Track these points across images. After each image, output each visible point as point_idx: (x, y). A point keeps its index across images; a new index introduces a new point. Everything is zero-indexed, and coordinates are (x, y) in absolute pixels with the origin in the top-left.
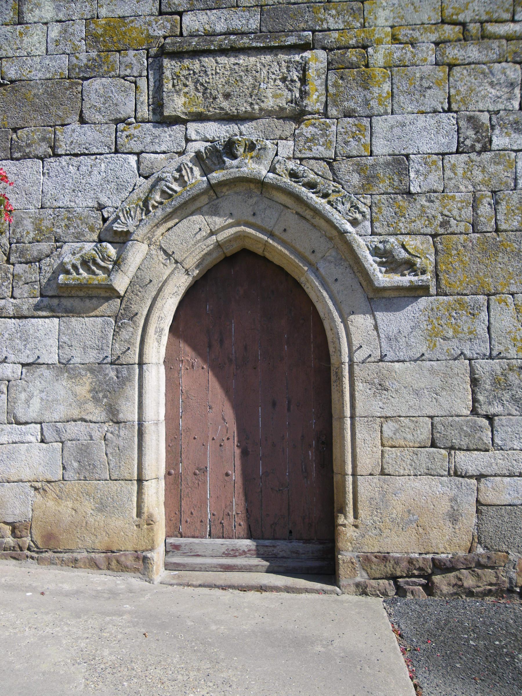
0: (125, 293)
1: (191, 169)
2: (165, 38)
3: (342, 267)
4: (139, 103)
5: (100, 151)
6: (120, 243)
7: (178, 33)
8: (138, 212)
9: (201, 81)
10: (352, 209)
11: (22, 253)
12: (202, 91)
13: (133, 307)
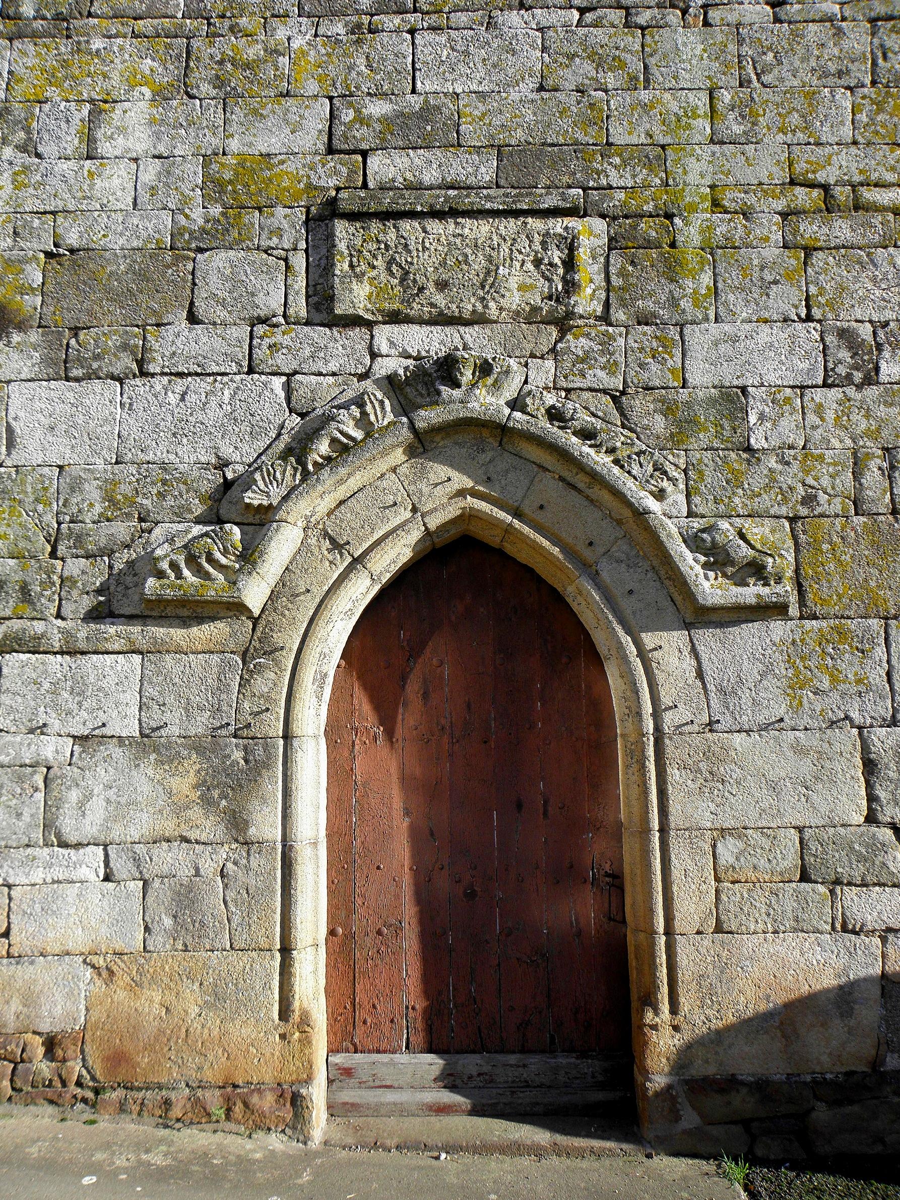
0: (263, 611)
1: (382, 403)
2: (338, 189)
3: (640, 570)
4: (291, 292)
5: (223, 370)
6: (255, 525)
7: (360, 184)
8: (287, 473)
9: (398, 260)
10: (657, 473)
11: (79, 540)
12: (398, 276)
13: (275, 635)
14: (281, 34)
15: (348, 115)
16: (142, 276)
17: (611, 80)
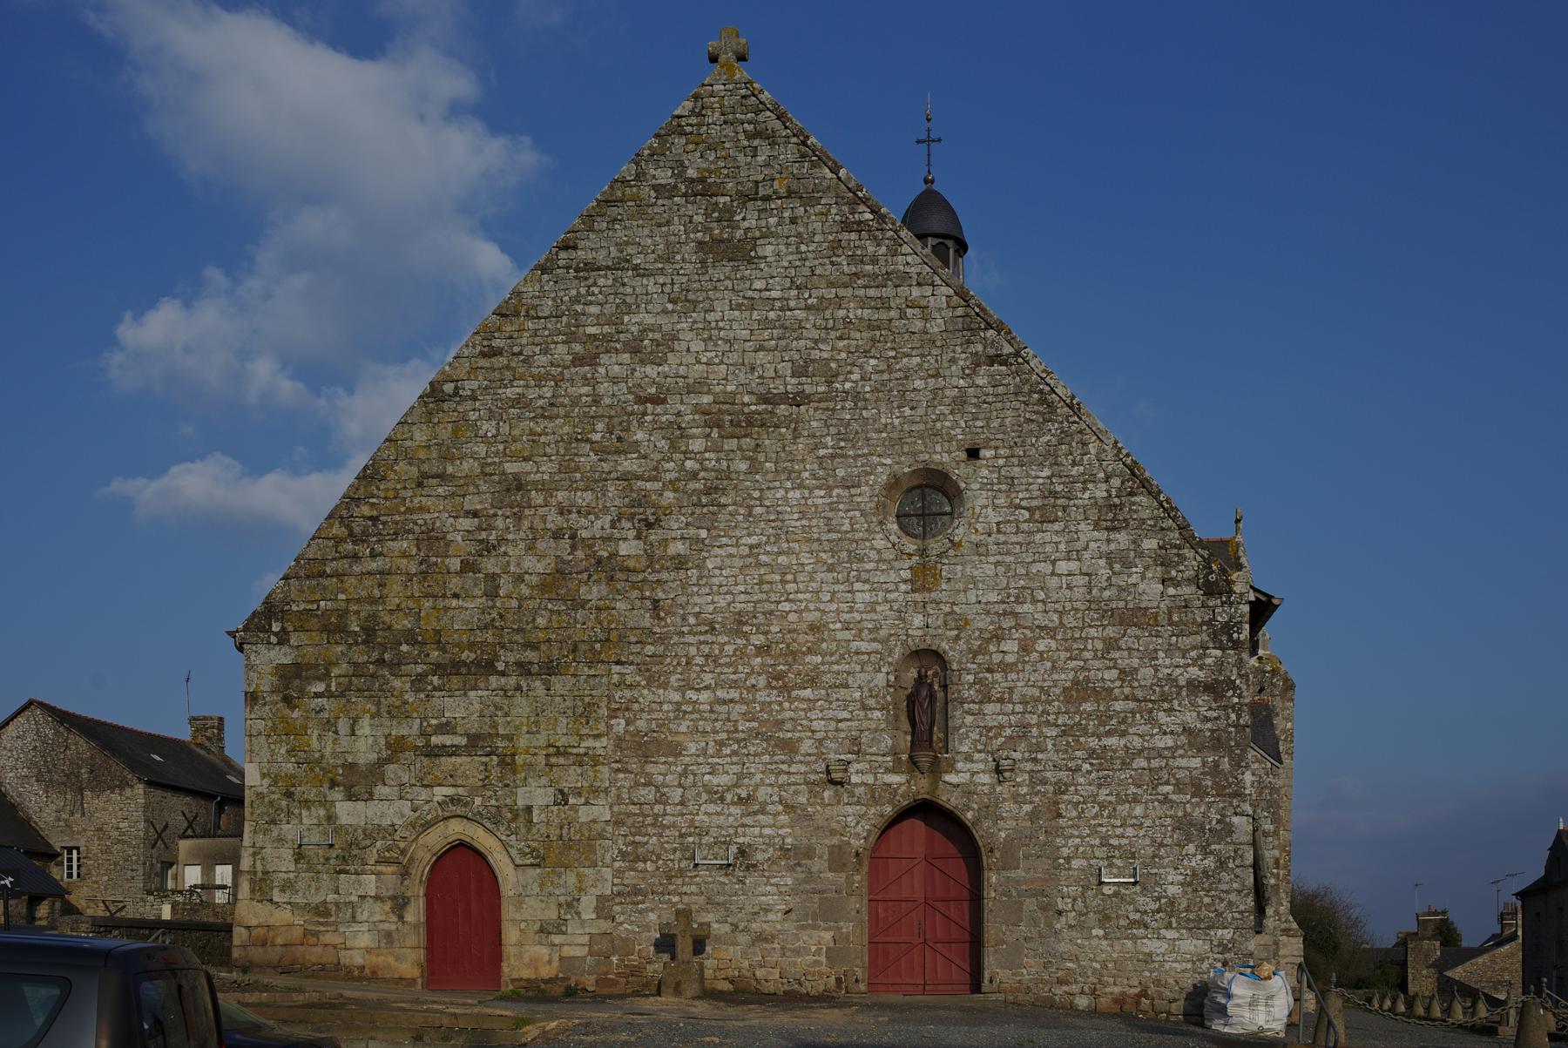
11: (357, 845)
14: (406, 697)
15: (425, 724)
16: (370, 771)
17: (499, 713)
